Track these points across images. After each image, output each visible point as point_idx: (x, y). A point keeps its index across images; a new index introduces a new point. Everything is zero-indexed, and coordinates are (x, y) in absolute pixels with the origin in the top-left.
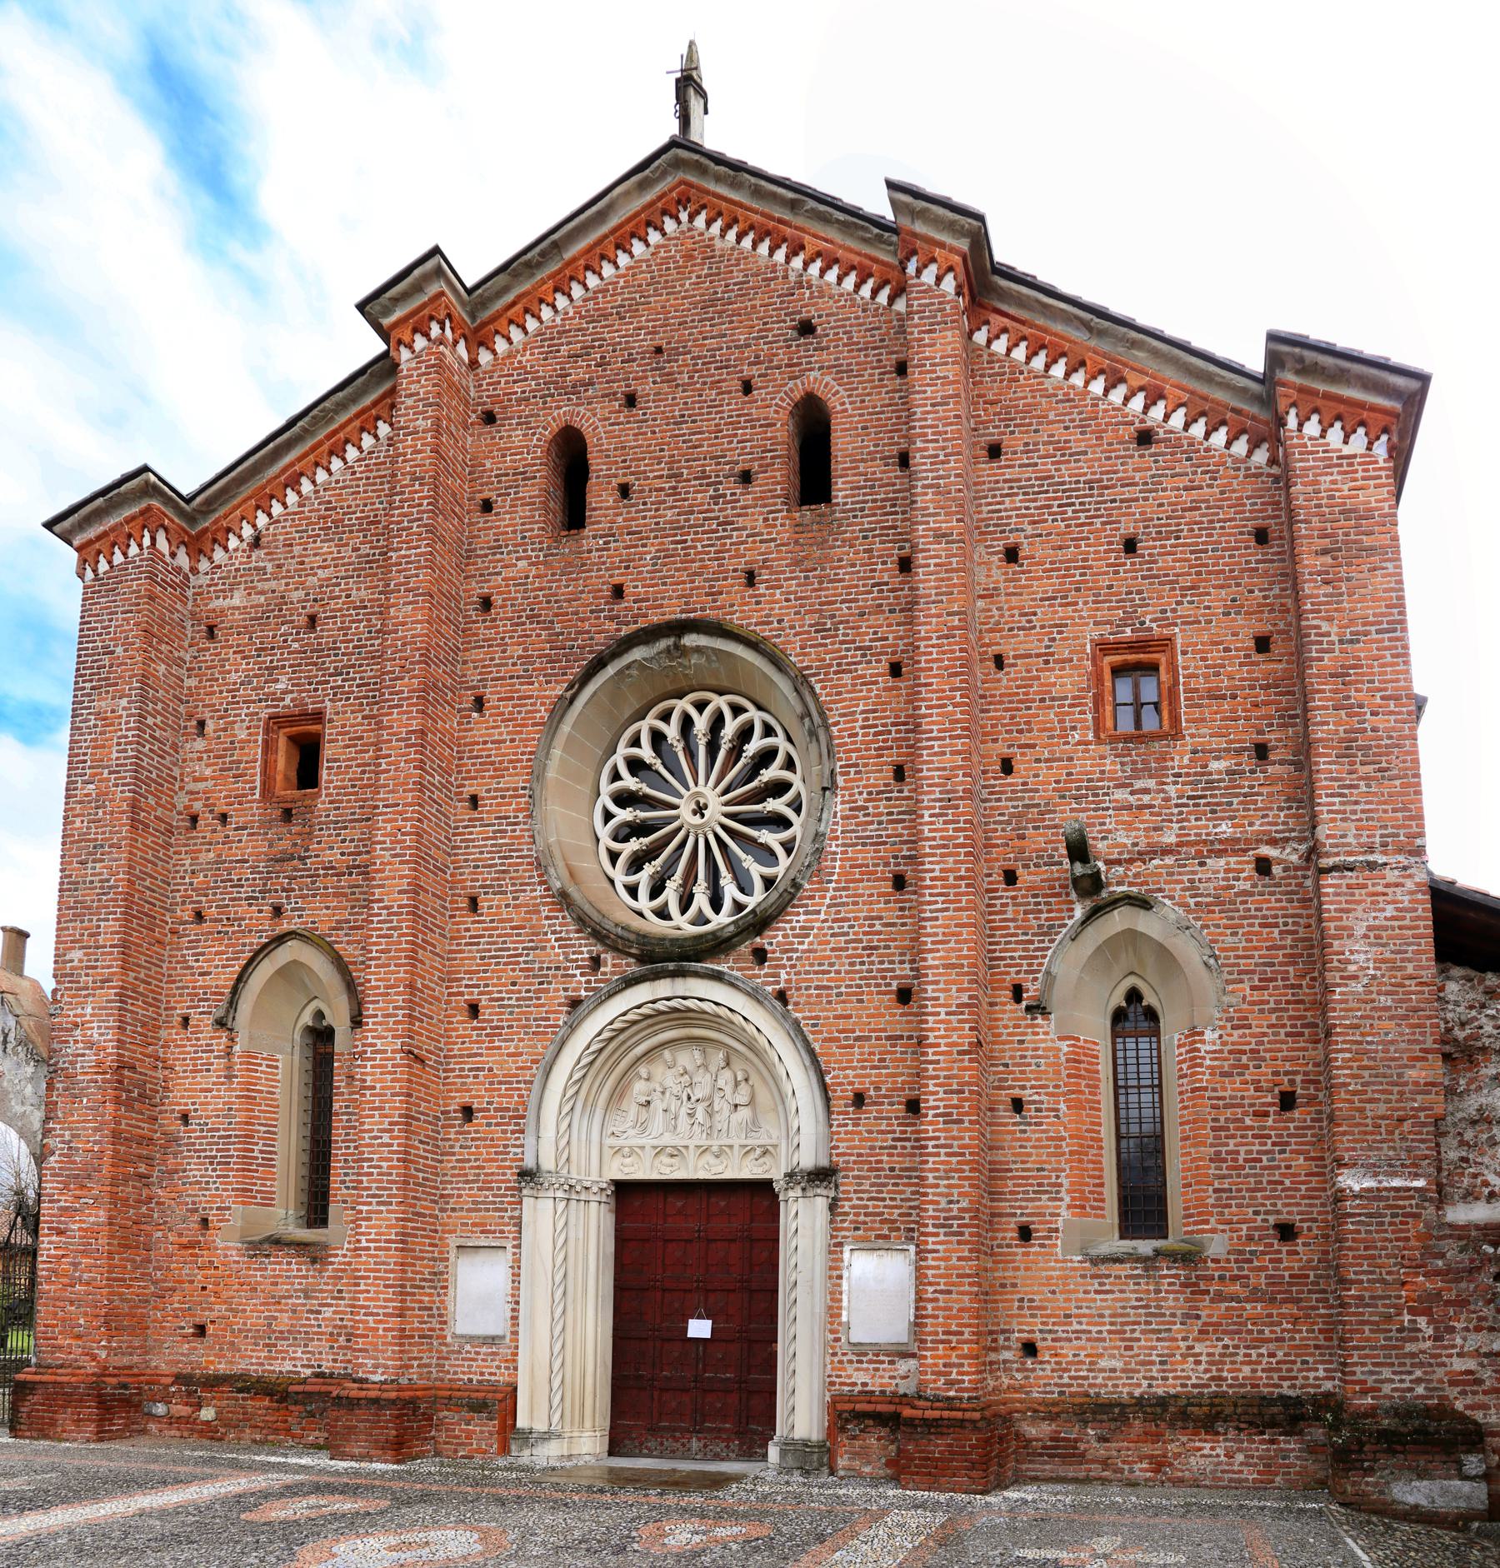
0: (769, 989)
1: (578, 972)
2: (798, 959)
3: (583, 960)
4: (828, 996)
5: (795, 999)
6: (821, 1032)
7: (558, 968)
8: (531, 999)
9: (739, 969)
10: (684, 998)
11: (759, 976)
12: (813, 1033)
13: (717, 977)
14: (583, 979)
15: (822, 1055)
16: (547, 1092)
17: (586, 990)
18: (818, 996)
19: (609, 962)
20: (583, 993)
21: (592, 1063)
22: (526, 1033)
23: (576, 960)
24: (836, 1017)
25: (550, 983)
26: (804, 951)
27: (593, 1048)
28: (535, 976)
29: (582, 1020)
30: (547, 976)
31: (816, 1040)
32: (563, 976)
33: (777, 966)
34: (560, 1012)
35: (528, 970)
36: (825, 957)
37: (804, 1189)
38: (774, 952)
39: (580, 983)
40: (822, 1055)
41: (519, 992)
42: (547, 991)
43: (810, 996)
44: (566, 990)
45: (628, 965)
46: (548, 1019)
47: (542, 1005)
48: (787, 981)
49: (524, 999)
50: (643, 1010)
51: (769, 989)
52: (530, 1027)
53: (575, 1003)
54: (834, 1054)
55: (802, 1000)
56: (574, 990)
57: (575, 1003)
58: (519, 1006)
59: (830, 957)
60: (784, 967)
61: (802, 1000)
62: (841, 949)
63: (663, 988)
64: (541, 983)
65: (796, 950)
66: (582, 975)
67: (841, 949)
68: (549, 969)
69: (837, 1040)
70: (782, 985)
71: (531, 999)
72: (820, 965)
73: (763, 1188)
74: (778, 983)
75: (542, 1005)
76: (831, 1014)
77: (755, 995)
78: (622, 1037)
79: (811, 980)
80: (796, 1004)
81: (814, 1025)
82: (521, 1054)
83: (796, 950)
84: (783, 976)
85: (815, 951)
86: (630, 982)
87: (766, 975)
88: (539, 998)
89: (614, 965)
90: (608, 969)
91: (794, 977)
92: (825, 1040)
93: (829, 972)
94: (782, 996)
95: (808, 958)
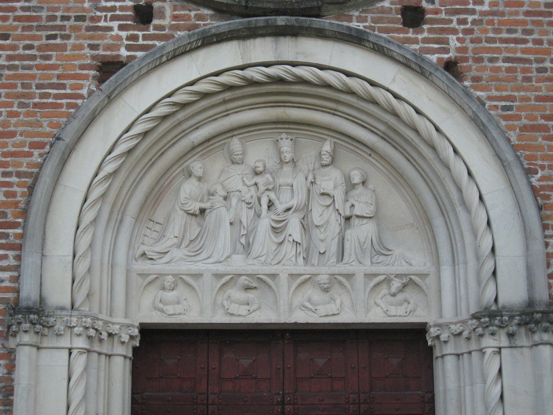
0: (434, 58)
1: (115, 24)
2: (474, 22)
3: (122, 8)
4: (524, 70)
5: (474, 73)
6: (519, 118)
7: (80, 18)
8: (33, 58)
9: (381, 30)
10: (294, 64)
11: (416, 41)
12: (505, 118)
13: (356, 39)
14: (124, 34)
15: (523, 148)
16: (60, 190)
17: (129, 48)
18: (508, 70)
19: (168, 12)
20: (124, 52)
21: (130, 152)
22: (22, 105)
23: (113, 9)
24: (539, 99)
25: (68, 37)
26: (483, 13)
27: (138, 129)
28: (39, 28)
29: (126, 89)
30: (62, 28)
31: (511, 128)
32: (88, 29)
33: (443, 31)
34: (86, 77)
35: (29, 19)
36: (517, 23)
37: (511, 336)
38: (437, 12)
39: (118, 38)
40: (523, 148)
41: (14, 48)
42: (63, 48)
43: (499, 69)
44: (93, 47)
45: (200, 17)
46: (63, 87)
47: (54, 67)
48: (458, 50)
49: (21, 58)
50: (222, 79)
51: (434, 58)
52: (31, 96)
53: (108, 68)
54: (540, 148)
55: (486, 74)
56: (108, 48)
57: (108, 68)
58: (10, 68)
59: (524, 23)
60: (454, 31)
61: (486, 74)
62: (541, 14)
63: (261, 50)
64: (54, 37)
65: (473, 12)
66: (122, 28)
67: (541, 14)
68: (63, 18)
69: (545, 129)
70: (452, 55)
71: (33, 58)
72: (509, 31)
73: (411, 342)
74: (447, 51)
75: (54, 67)
76: (532, 95)
77: (416, 67)
78: (181, 116)
79: (498, 50)
80: (476, 79)
81: (505, 108)
82: (13, 134)
83: (473, 12)
84: (453, 42)
85: (503, 14)
86: (209, 40)
87: (425, 40)
88: (48, 58)
89: (175, 18)
90: (166, 22)
91: (471, 46)
92: (524, 128)
93: (525, 41)
94: (450, 66)
95: (491, 22)
